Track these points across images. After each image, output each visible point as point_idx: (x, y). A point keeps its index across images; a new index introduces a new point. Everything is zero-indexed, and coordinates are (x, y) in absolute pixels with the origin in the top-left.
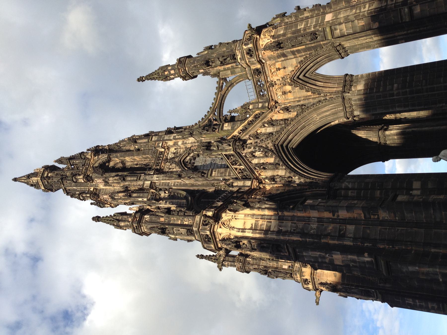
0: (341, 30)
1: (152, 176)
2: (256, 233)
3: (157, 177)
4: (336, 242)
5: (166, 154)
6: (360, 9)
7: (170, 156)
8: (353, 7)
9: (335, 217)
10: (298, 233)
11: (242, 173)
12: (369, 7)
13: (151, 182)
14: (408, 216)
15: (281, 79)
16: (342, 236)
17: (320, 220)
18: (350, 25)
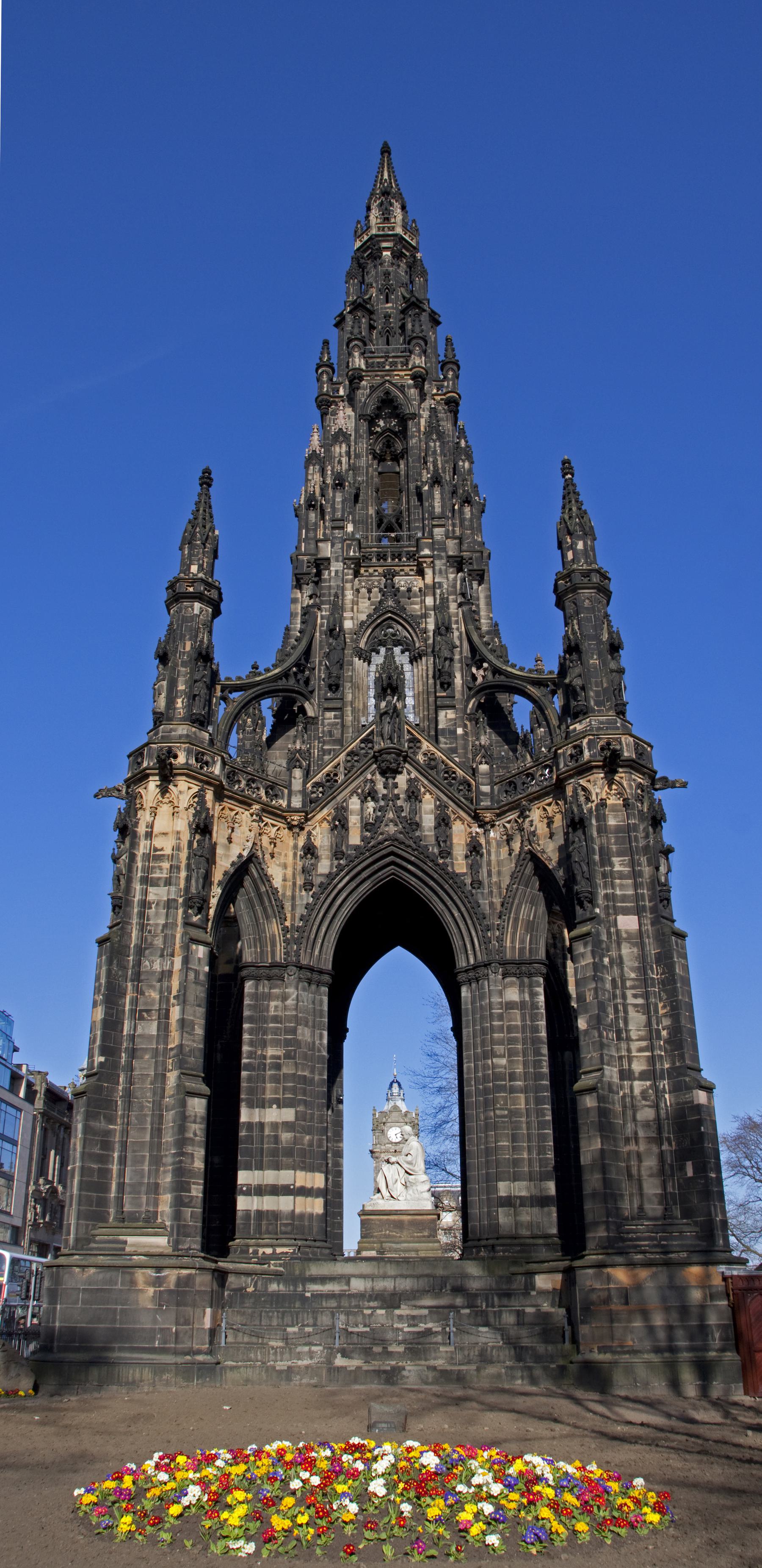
0: (583, 955)
1: (341, 559)
2: (143, 861)
3: (337, 572)
4: (127, 1008)
5: (407, 569)
6: (632, 987)
7: (401, 581)
8: (643, 970)
9: (172, 1001)
10: (142, 939)
11: (328, 781)
12: (635, 1006)
13: (328, 559)
14: (169, 1116)
15: (532, 829)
16: (138, 1015)
17: (166, 975)
18: (590, 973)
